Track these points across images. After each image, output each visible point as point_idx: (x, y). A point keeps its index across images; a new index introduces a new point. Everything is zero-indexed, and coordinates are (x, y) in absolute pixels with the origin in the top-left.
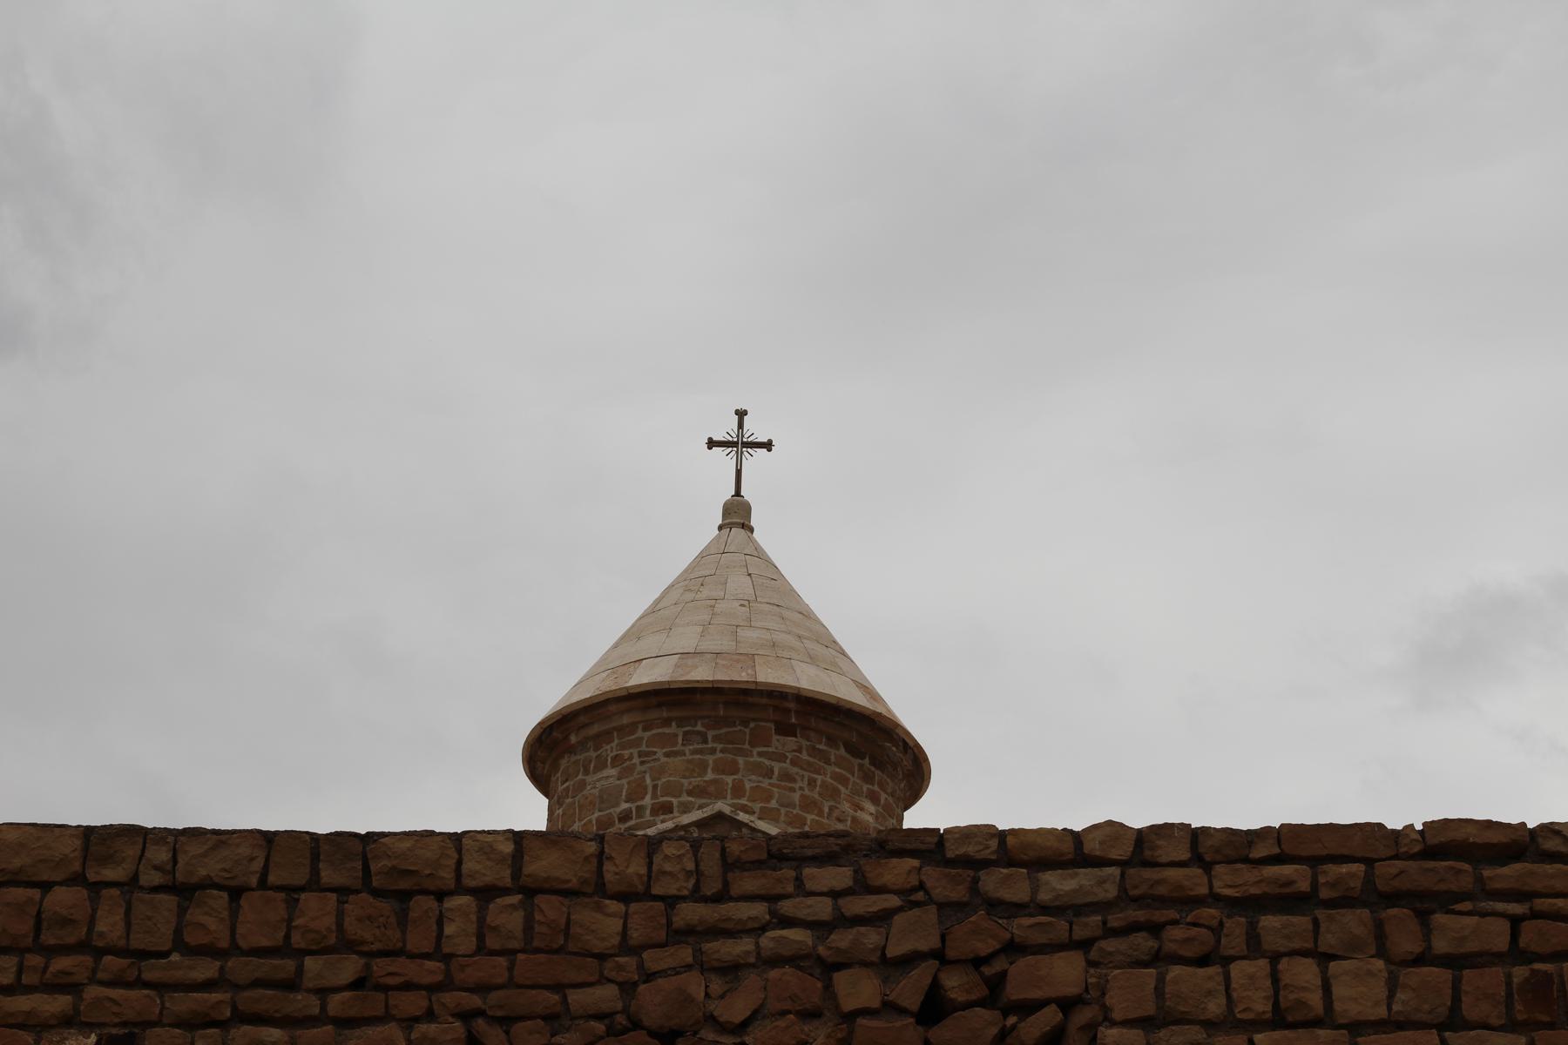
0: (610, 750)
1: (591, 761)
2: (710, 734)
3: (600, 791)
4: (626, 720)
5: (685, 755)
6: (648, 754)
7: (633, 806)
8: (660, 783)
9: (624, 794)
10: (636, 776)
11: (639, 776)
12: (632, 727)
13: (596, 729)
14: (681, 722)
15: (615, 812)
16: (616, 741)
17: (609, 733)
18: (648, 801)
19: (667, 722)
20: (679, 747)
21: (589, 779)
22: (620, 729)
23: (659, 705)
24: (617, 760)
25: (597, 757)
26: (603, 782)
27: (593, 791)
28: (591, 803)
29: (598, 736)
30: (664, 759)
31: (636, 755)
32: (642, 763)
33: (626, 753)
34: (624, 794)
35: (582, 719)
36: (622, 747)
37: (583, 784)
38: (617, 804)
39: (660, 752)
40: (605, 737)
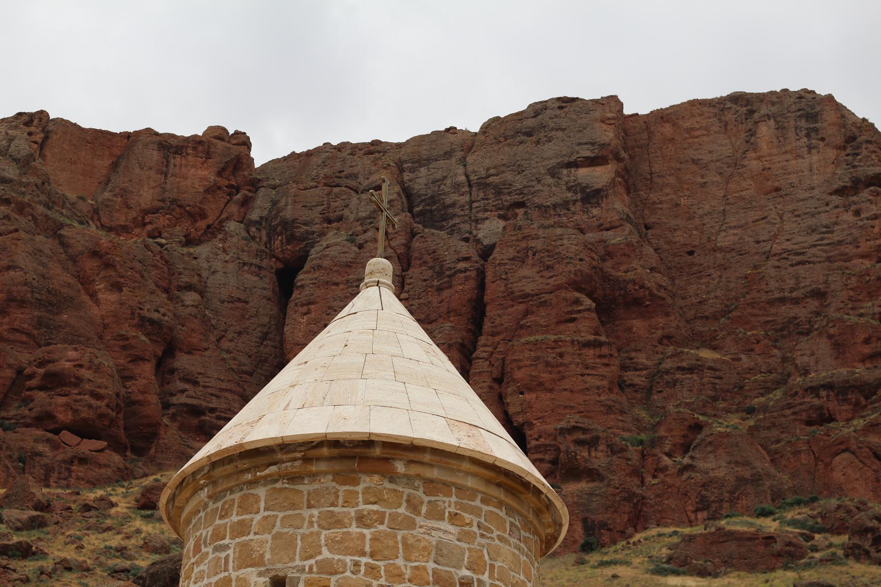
0: (449, 503)
1: (422, 503)
2: (523, 533)
3: (439, 543)
4: (470, 482)
5: (510, 545)
6: (488, 529)
7: (475, 577)
8: (497, 564)
9: (466, 559)
10: (475, 546)
11: (478, 547)
12: (472, 493)
13: (434, 473)
14: (510, 511)
15: (457, 574)
16: (454, 499)
17: (446, 485)
18: (485, 577)
19: (500, 504)
20: (506, 536)
21: (419, 520)
22: (460, 488)
23: (499, 485)
24: (454, 518)
25: (430, 502)
26: (441, 534)
27: (427, 537)
28: (425, 548)
29: (431, 481)
30: (497, 542)
31: (475, 524)
32: (482, 536)
33: (467, 517)
34: (466, 559)
35: (427, 458)
36: (464, 508)
37: (412, 525)
38: (460, 568)
39: (496, 533)
40: (445, 487)
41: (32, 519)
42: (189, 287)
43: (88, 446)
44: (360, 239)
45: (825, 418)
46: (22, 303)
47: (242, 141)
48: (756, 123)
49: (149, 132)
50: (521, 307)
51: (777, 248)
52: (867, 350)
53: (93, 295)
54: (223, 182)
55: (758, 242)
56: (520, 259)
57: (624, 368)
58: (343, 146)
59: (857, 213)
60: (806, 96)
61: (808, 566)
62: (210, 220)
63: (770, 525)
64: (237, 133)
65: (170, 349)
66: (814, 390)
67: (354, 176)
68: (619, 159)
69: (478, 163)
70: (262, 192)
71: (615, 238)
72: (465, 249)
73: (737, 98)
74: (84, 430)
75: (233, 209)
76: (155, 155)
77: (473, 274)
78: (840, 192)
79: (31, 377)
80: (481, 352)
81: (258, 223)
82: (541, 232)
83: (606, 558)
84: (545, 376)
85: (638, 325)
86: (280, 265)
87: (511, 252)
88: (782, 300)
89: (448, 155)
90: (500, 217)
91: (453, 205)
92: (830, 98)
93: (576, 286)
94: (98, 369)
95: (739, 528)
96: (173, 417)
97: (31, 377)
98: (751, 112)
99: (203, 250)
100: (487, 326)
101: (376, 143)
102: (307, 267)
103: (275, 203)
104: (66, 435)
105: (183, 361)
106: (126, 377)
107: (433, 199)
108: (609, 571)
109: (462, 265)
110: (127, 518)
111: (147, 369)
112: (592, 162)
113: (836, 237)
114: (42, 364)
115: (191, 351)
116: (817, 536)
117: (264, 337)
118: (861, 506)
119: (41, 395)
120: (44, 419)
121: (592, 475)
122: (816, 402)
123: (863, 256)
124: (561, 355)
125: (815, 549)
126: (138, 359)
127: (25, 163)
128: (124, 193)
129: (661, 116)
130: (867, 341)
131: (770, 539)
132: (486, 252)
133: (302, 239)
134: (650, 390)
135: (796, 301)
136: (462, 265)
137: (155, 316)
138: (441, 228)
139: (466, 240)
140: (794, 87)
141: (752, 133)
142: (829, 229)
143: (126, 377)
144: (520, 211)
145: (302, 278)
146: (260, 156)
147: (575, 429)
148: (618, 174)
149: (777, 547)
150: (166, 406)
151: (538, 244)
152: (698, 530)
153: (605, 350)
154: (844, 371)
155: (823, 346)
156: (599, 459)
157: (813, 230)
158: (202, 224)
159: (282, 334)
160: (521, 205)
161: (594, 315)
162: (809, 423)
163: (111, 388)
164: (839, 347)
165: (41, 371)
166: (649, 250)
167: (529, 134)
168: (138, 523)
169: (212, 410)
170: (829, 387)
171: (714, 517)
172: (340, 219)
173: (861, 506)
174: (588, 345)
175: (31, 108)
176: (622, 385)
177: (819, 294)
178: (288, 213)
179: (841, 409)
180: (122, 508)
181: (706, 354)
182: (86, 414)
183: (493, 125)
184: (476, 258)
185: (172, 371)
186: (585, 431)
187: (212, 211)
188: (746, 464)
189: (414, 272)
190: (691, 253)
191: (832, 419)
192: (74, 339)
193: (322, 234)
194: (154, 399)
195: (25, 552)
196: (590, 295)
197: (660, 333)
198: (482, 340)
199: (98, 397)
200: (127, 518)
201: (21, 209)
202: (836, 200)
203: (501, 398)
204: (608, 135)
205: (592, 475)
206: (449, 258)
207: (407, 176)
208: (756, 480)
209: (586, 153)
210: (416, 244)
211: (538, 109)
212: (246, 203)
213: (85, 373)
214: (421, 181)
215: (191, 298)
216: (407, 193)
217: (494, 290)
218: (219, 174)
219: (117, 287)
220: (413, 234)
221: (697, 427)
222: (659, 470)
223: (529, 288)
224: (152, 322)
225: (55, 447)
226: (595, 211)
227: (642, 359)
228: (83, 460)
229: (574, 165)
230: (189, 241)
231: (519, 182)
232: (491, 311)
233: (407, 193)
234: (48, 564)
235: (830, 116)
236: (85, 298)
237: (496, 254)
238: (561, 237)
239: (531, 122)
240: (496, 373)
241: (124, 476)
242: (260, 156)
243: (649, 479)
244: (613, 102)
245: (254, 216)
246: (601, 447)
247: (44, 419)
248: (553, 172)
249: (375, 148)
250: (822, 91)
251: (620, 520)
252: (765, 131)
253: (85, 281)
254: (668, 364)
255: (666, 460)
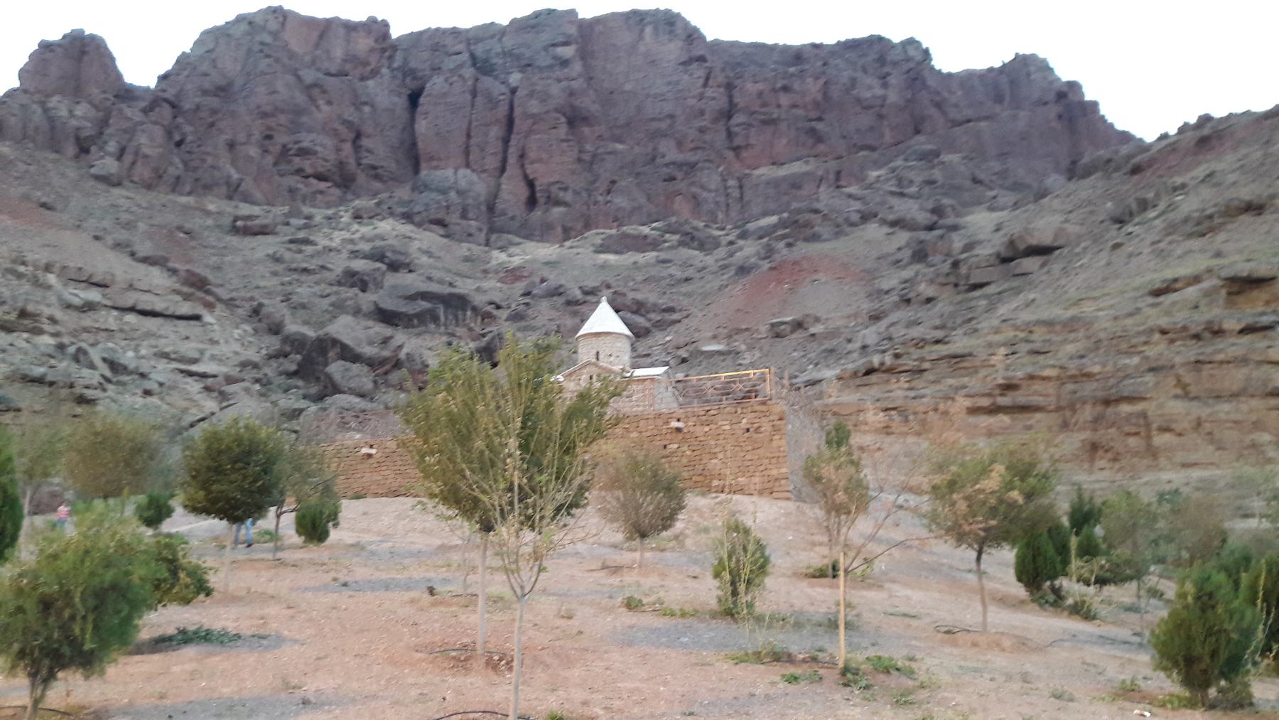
41: (305, 224)
42: (366, 103)
43: (323, 185)
44: (451, 80)
45: (672, 179)
46: (283, 111)
47: (385, 25)
48: (645, 25)
49: (337, 19)
50: (530, 121)
51: (652, 92)
52: (692, 146)
53: (317, 107)
54: (379, 46)
55: (643, 89)
56: (531, 95)
57: (580, 152)
58: (437, 30)
59: (691, 75)
60: (667, 12)
61: (661, 250)
62: (372, 66)
63: (645, 230)
64: (383, 21)
65: (358, 136)
66: (667, 165)
67: (444, 46)
68: (577, 43)
69: (508, 42)
70: (398, 53)
71: (575, 85)
72: (503, 89)
73: (635, 13)
74: (321, 177)
75: (384, 61)
76: (342, 31)
77: (507, 101)
78: (684, 63)
79: (290, 149)
80: (513, 142)
81: (397, 69)
82: (540, 82)
83: (574, 244)
84: (544, 156)
85: (586, 130)
86: (409, 92)
87: (525, 92)
88: (653, 119)
89: (493, 37)
90: (520, 71)
91: (495, 64)
92: (678, 15)
93: (557, 110)
94: (324, 146)
95: (632, 232)
96: (363, 171)
97: (290, 149)
98: (642, 20)
99: (371, 83)
100: (515, 130)
101: (454, 28)
102: (425, 94)
103: (405, 59)
104: (312, 181)
105: (365, 142)
106: (338, 150)
107: (486, 61)
108: (575, 251)
109: (502, 97)
110: (349, 224)
111: (348, 147)
112: (566, 44)
113: (680, 88)
114: (296, 142)
115: (369, 136)
116: (667, 236)
117: (404, 129)
118: (686, 222)
119: (297, 160)
120: (299, 171)
121: (566, 204)
122: (668, 171)
123: (693, 97)
124: (551, 146)
125: (665, 241)
126: (343, 141)
127: (275, 35)
128: (328, 52)
129: (597, 21)
130: (692, 141)
131: (646, 237)
132: (514, 91)
133: (421, 78)
134: (592, 163)
135: (660, 120)
136: (502, 97)
137: (351, 118)
138: (490, 76)
139: (503, 83)
140: (662, 8)
141: (642, 31)
142: (677, 83)
143: (338, 150)
144: (529, 68)
145: (422, 100)
146: (395, 33)
147: (557, 182)
148: (577, 51)
149: (649, 241)
150: (359, 164)
151: (538, 88)
152: (613, 231)
153: (571, 143)
154: (682, 156)
155: (672, 144)
156: (568, 197)
157: (669, 83)
158: (369, 68)
159: (413, 129)
160: (529, 65)
161: (565, 125)
162: (665, 180)
163: (332, 157)
164: (680, 144)
165: (296, 146)
166: (591, 92)
167: (533, 27)
168: (356, 227)
169: (382, 167)
170: (674, 163)
171: (620, 225)
172: (439, 68)
173: (686, 222)
174: (563, 141)
175: (275, 4)
176: (579, 160)
177: (672, 116)
178: (413, 64)
179: (679, 175)
180: (346, 218)
181: (619, 147)
182: (321, 169)
183: (514, 22)
184: (509, 94)
185: (361, 146)
186: (563, 183)
187: (373, 61)
188: (634, 200)
189: (479, 100)
190: (611, 93)
191: (674, 179)
192: (310, 130)
193: (431, 77)
194: (352, 161)
195: (307, 242)
196: (564, 114)
197: (597, 134)
198: (513, 136)
199: (326, 161)
200: (349, 224)
201: (277, 60)
202: (681, 68)
203: (522, 166)
204: (573, 30)
205: (566, 204)
206: (496, 93)
207: (472, 47)
208: (640, 208)
209: (561, 39)
210: (479, 85)
211: (537, 15)
212: (391, 58)
213: (318, 149)
214: (479, 50)
215: (367, 109)
216: (473, 57)
217: (518, 112)
218: (376, 41)
219: (329, 103)
220: (477, 80)
221: (613, 182)
222: (596, 203)
223: (535, 111)
224: (349, 122)
225: (306, 186)
226: (566, 70)
227: (588, 147)
228: (321, 192)
229: (554, 45)
230: (363, 79)
231: (528, 53)
232: (517, 121)
233: (473, 57)
234: (319, 248)
235: (679, 24)
236: (313, 108)
237: (520, 93)
238: (550, 85)
239: (533, 22)
240: (520, 153)
241: (342, 201)
242: (395, 33)
243: (592, 207)
244: (572, 13)
245: (395, 65)
246: (570, 191)
247: (299, 171)
248: (545, 49)
249: (455, 32)
250: (676, 10)
251: (579, 226)
252: (648, 30)
253: (313, 100)
254: (600, 151)
255: (600, 198)
